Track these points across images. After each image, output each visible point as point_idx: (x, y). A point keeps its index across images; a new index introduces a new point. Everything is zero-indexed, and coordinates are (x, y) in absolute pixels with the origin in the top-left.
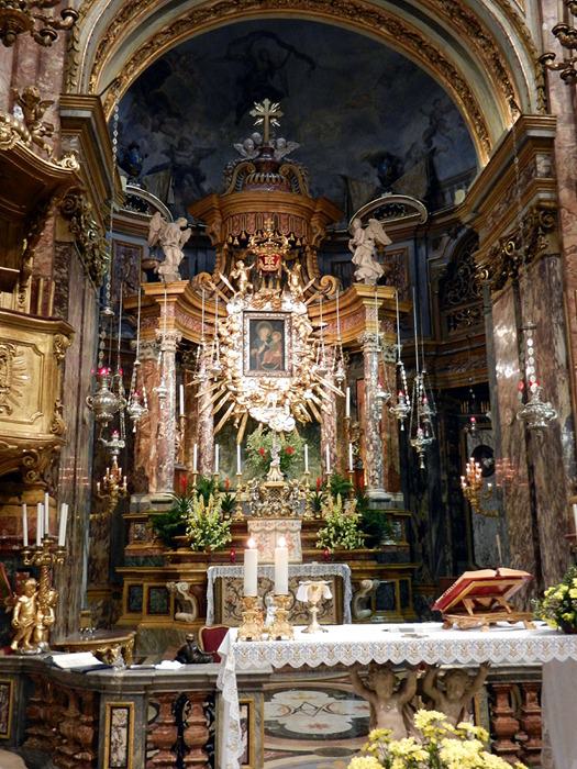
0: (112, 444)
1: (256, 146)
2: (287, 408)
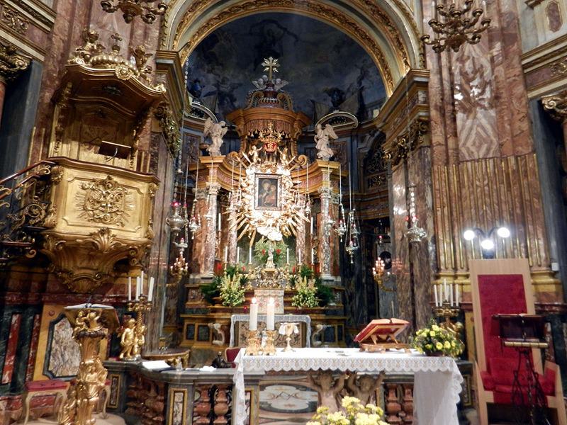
0: (180, 245)
1: (264, 82)
2: (278, 228)
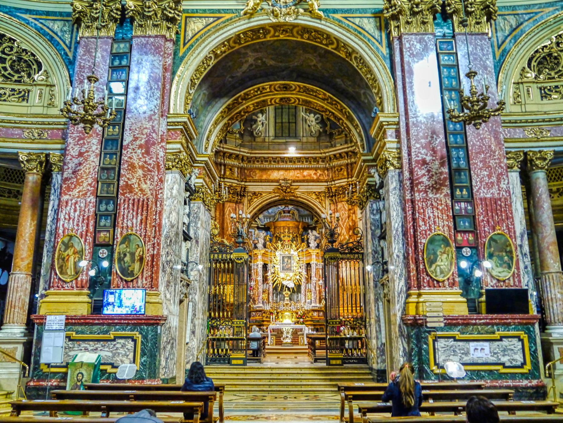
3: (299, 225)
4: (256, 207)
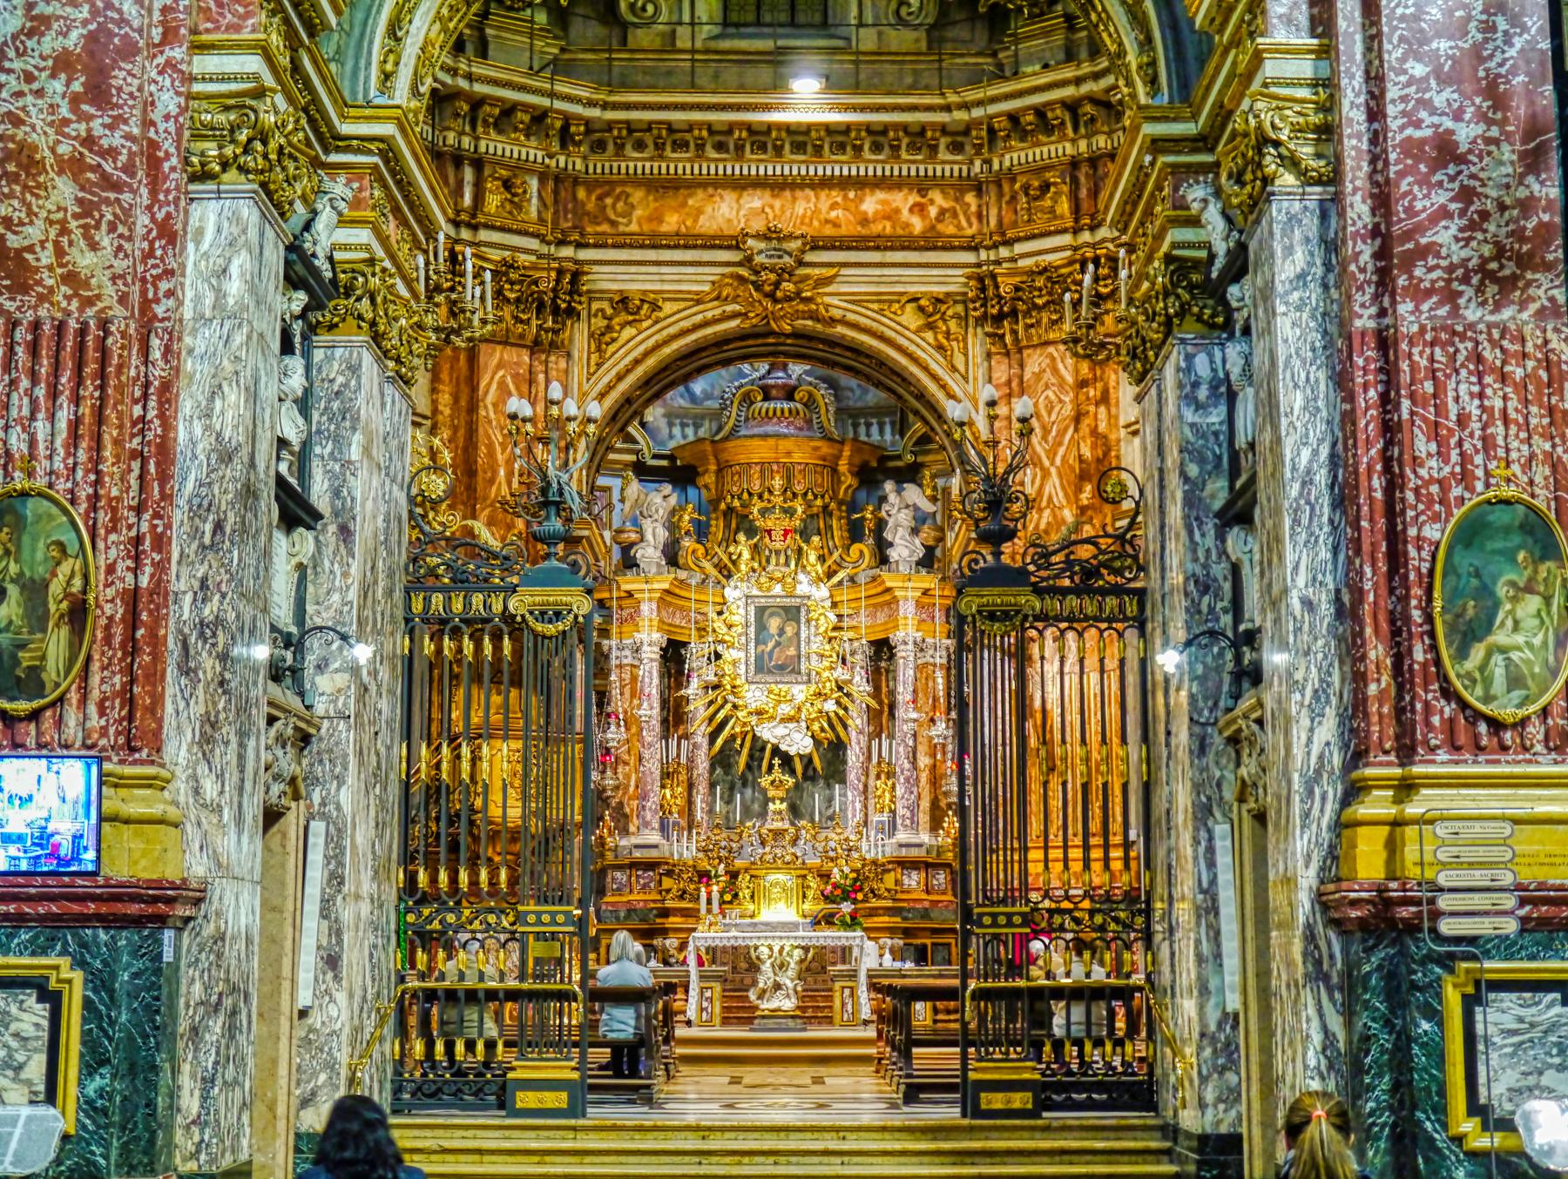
2: (804, 725)
3: (838, 457)
4: (628, 371)
